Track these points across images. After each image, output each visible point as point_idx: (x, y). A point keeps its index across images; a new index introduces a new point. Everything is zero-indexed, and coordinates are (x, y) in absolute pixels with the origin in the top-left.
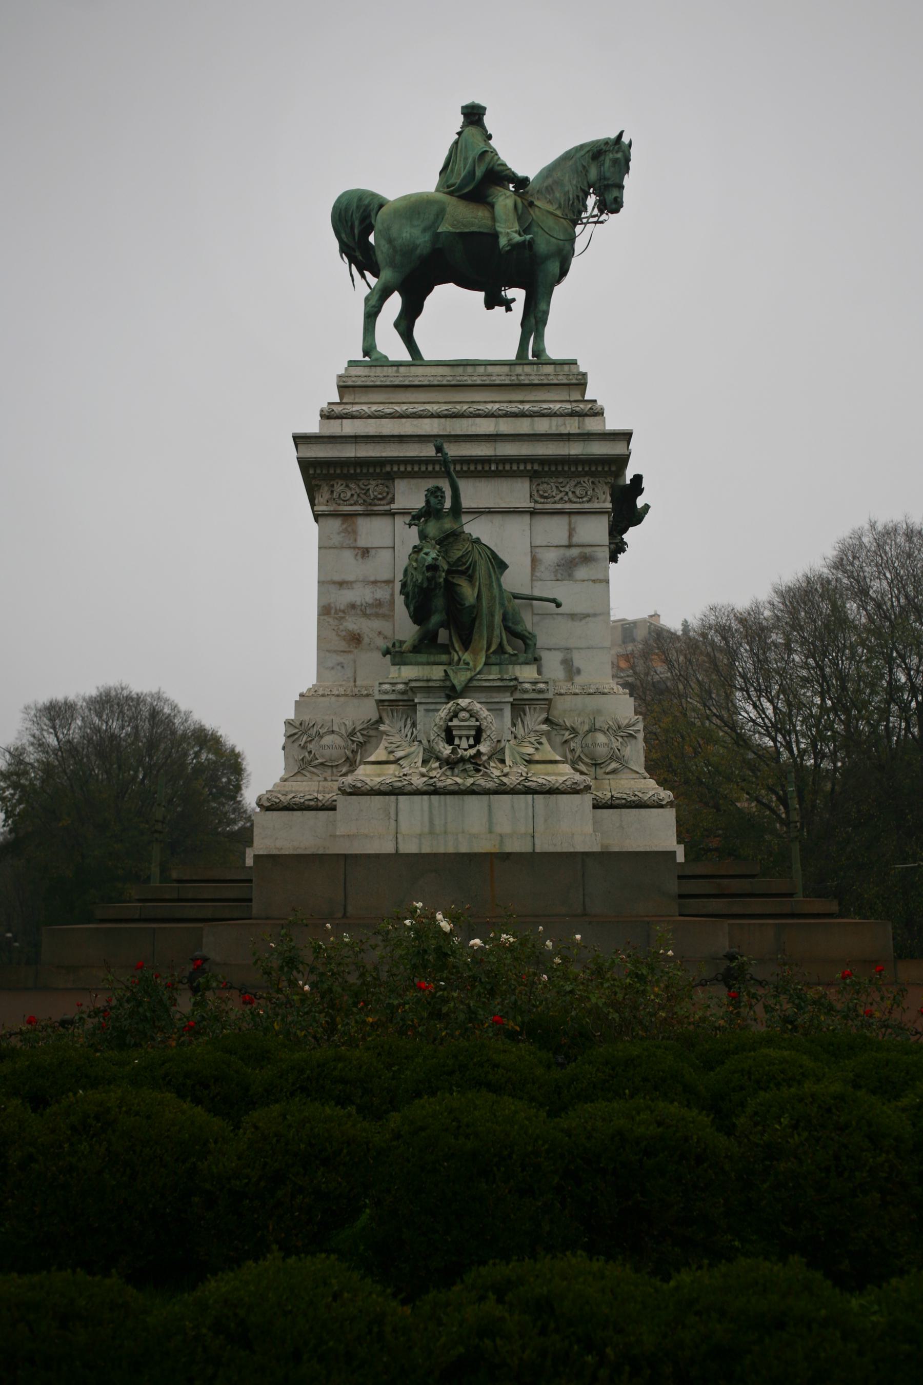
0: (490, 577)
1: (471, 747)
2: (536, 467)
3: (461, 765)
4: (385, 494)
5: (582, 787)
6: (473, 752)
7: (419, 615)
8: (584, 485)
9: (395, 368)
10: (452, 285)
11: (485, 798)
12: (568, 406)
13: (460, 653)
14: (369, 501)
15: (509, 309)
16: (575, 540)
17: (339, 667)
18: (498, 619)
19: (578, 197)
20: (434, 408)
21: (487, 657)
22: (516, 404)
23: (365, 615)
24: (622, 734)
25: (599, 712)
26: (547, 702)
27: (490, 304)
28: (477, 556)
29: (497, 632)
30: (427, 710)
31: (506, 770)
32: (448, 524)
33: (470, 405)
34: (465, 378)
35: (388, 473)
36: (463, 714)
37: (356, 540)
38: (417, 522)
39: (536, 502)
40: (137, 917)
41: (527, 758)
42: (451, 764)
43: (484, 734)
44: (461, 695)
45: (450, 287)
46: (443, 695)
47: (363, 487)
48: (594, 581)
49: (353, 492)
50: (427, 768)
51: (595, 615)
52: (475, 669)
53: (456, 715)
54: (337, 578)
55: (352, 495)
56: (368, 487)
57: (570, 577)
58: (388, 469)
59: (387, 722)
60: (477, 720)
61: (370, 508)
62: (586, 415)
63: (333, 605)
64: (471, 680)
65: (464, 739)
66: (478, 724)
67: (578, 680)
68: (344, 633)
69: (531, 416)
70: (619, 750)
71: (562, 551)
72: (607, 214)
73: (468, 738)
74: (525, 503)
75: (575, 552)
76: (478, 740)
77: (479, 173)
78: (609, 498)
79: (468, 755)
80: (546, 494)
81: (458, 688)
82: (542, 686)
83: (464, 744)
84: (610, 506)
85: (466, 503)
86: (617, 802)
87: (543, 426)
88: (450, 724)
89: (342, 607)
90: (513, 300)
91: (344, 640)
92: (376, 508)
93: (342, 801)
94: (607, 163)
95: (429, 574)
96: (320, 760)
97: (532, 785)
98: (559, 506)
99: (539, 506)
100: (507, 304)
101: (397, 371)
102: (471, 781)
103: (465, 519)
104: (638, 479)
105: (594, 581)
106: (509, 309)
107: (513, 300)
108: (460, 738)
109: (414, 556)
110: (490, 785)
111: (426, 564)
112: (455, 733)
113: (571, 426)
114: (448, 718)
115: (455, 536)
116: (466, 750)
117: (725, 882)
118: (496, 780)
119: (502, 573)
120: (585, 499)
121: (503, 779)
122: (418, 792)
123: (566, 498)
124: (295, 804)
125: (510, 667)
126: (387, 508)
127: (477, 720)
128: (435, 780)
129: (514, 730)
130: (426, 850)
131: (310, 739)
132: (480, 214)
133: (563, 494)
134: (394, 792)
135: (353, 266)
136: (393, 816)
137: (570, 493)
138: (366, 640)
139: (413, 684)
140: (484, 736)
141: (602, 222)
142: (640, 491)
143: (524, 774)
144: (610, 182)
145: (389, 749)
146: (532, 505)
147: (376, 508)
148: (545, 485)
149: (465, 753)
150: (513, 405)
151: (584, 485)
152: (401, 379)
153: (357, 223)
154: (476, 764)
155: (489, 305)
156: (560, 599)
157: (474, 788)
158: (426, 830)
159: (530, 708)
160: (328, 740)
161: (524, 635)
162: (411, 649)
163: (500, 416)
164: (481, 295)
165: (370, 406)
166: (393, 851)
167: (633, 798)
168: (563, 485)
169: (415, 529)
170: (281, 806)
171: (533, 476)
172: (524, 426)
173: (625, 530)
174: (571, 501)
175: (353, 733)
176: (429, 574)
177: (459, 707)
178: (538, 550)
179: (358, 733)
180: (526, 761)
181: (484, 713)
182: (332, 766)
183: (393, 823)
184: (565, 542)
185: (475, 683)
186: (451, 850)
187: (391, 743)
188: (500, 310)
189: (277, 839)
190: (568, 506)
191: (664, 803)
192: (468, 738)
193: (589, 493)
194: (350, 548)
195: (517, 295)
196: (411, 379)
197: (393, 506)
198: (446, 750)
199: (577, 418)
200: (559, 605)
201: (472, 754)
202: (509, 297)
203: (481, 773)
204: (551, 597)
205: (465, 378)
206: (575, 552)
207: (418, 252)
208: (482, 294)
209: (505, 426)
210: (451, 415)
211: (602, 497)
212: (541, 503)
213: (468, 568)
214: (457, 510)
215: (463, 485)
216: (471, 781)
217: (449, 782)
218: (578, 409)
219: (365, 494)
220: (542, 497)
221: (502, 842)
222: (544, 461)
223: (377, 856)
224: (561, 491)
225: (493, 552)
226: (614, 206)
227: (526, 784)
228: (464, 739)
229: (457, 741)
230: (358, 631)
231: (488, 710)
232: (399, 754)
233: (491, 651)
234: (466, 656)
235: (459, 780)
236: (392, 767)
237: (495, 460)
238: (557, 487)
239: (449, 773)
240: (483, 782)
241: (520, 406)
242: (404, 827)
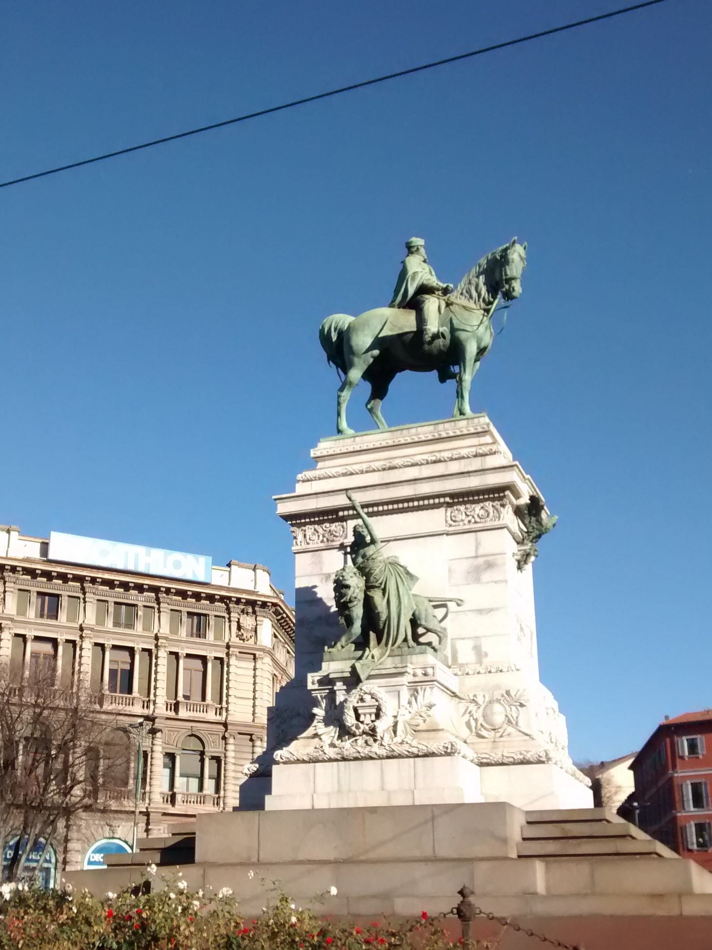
8: (486, 508)
9: (352, 439)
10: (398, 374)
11: (379, 761)
16: (481, 551)
21: (392, 650)
27: (442, 379)
37: (321, 569)
39: (451, 526)
40: (130, 863)
45: (407, 373)
47: (325, 529)
48: (496, 582)
51: (497, 609)
57: (478, 580)
61: (330, 543)
65: (368, 716)
66: (377, 704)
67: (486, 661)
71: (471, 561)
73: (371, 715)
74: (442, 527)
75: (481, 561)
76: (378, 716)
98: (467, 527)
101: (354, 441)
102: (368, 748)
105: (496, 582)
108: (365, 715)
110: (383, 752)
112: (360, 711)
113: (476, 464)
118: (387, 748)
122: (330, 760)
125: (409, 656)
130: (334, 805)
134: (315, 761)
135: (339, 369)
155: (442, 379)
156: (462, 598)
161: (436, 630)
163: (422, 464)
164: (435, 373)
166: (309, 807)
174: (476, 522)
177: (362, 691)
181: (381, 694)
183: (312, 784)
184: (473, 554)
192: (371, 715)
194: (317, 575)
199: (480, 458)
206: (481, 561)
209: (427, 471)
212: (454, 526)
221: (389, 799)
222: (452, 495)
225: (405, 568)
228: (368, 716)
231: (387, 692)
235: (360, 749)
240: (376, 748)
242: (319, 788)
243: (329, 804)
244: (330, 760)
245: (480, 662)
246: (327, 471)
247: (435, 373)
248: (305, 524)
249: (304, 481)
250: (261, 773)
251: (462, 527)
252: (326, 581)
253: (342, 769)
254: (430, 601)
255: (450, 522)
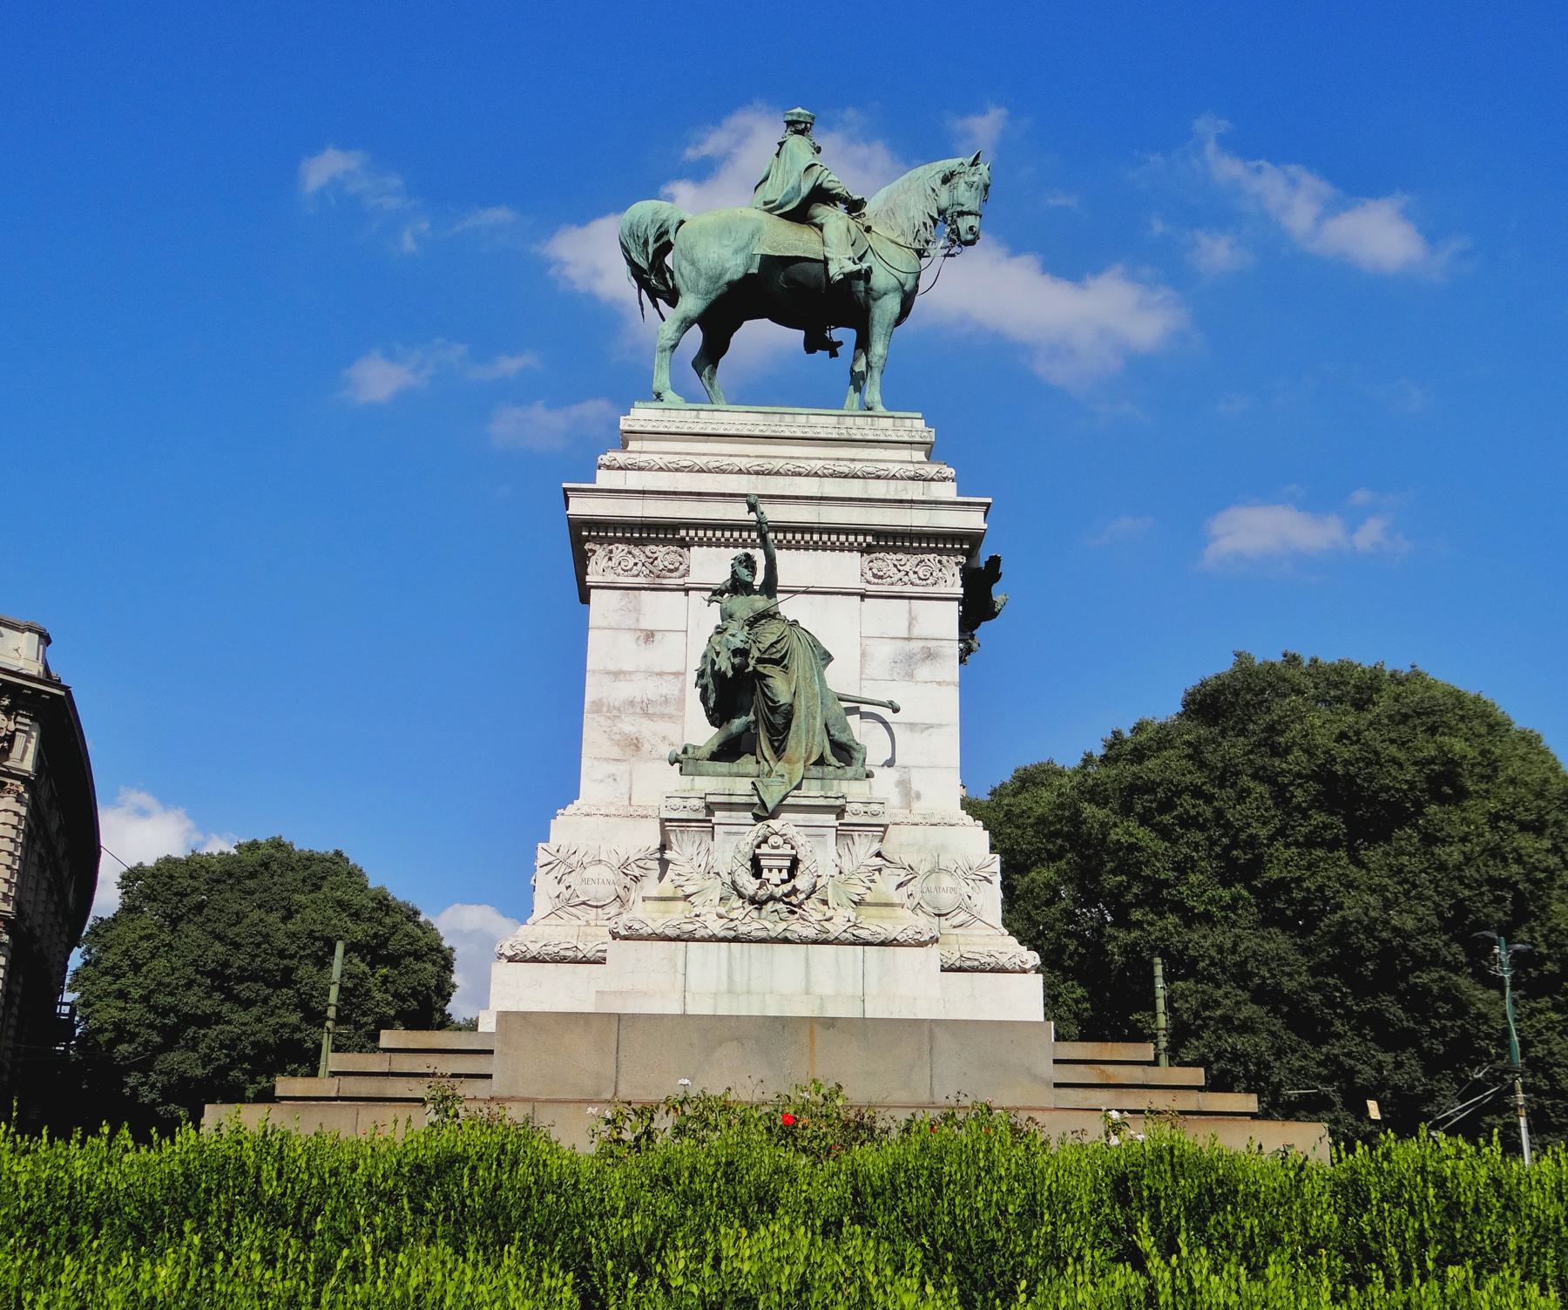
0: (812, 669)
1: (784, 882)
2: (869, 539)
3: (771, 904)
4: (677, 565)
5: (927, 938)
6: (787, 888)
7: (718, 715)
8: (929, 563)
10: (766, 320)
12: (910, 467)
13: (771, 763)
14: (656, 571)
15: (834, 354)
16: (916, 632)
17: (610, 780)
18: (819, 723)
19: (925, 224)
20: (743, 463)
22: (846, 463)
23: (646, 714)
24: (974, 877)
25: (944, 848)
26: (882, 829)
28: (795, 643)
29: (817, 739)
30: (729, 833)
31: (829, 913)
32: (760, 603)
33: (788, 461)
34: (782, 429)
35: (683, 539)
36: (772, 840)
37: (638, 620)
38: (719, 598)
39: (868, 582)
41: (856, 899)
42: (758, 903)
43: (800, 866)
44: (774, 815)
46: (749, 815)
47: (650, 555)
48: (939, 683)
49: (637, 561)
50: (727, 908)
51: (940, 726)
52: (791, 784)
53: (765, 841)
54: (612, 667)
55: (636, 564)
56: (655, 555)
57: (910, 676)
58: (683, 533)
59: (675, 847)
60: (793, 848)
61: (658, 581)
62: (932, 480)
63: (605, 701)
64: (785, 797)
65: (775, 871)
66: (794, 852)
67: (917, 806)
68: (618, 737)
69: (864, 478)
70: (970, 897)
71: (900, 643)
72: (959, 246)
73: (780, 871)
74: (857, 584)
75: (916, 646)
76: (792, 872)
77: (805, 190)
78: (960, 582)
79: (781, 893)
80: (881, 574)
81: (770, 806)
82: (875, 807)
83: (775, 877)
84: (961, 591)
85: (783, 580)
86: (969, 963)
87: (878, 489)
88: (757, 851)
89: (617, 704)
90: (840, 343)
91: (618, 745)
92: (664, 581)
93: (615, 949)
94: (962, 187)
95: (737, 661)
96: (582, 899)
97: (864, 934)
98: (897, 588)
99: (869, 587)
100: (832, 348)
101: (697, 417)
102: (783, 925)
103: (780, 597)
104: (994, 562)
105: (939, 683)
106: (834, 354)
107: (840, 343)
108: (770, 870)
109: (718, 638)
110: (810, 933)
111: (732, 648)
112: (763, 863)
114: (755, 843)
115: (769, 615)
116: (777, 886)
117: (1110, 1069)
119: (825, 666)
120: (928, 582)
121: (826, 924)
122: (714, 939)
123: (906, 579)
124: (547, 954)
125: (836, 782)
126: (681, 581)
127: (793, 848)
128: (736, 922)
129: (838, 862)
130: (723, 1010)
131: (568, 870)
132: (806, 236)
133: (904, 573)
136: (681, 969)
137: (911, 573)
138: (646, 747)
139: (710, 799)
140: (801, 866)
141: (953, 255)
142: (997, 577)
143: (852, 919)
144: (965, 209)
145: (677, 883)
146: (864, 585)
147: (664, 581)
148: (880, 562)
149: (776, 889)
150: (841, 463)
151: (929, 563)
152: (702, 425)
153: (651, 240)
154: (790, 903)
155: (810, 346)
156: (897, 702)
157: (788, 935)
158: (724, 987)
159: (859, 835)
160: (592, 872)
162: (708, 756)
164: (800, 335)
165: (661, 456)
166: (679, 1011)
167: (988, 960)
168: (903, 563)
169: (716, 607)
170: (528, 957)
171: (867, 550)
172: (855, 488)
173: (976, 627)
175: (625, 866)
176: (737, 661)
177: (769, 829)
178: (869, 642)
179: (633, 864)
180: (855, 903)
181: (800, 839)
182: (597, 907)
183: (680, 978)
185: (789, 801)
186: (755, 1012)
187: (679, 875)
188: (822, 355)
189: (521, 999)
190: (909, 589)
191: (1027, 966)
192: (780, 871)
193: (934, 574)
195: (844, 335)
196: (714, 426)
197: (687, 579)
198: (750, 885)
200: (896, 710)
201: (786, 891)
202: (835, 339)
203: (797, 916)
204: (885, 700)
205: (782, 429)
206: (916, 646)
207: (727, 278)
208: (801, 334)
210: (763, 472)
211: (950, 579)
213: (783, 657)
214: (770, 587)
215: (782, 557)
216: (783, 925)
217: (755, 925)
218: (922, 472)
219: (652, 563)
220: (875, 576)
221: (822, 1007)
223: (661, 1017)
224: (899, 571)
225: (814, 639)
226: (970, 237)
227: (855, 932)
228: (775, 871)
229: (765, 874)
230: (637, 735)
232: (689, 890)
233: (811, 762)
234: (780, 767)
236: (681, 905)
237: (819, 528)
238: (895, 566)
239: (755, 914)
240: (798, 928)
241: (852, 466)
243: (715, 1011)
244: (714, 939)
245: (909, 806)
246: (656, 457)
247: (800, 335)
248: (612, 541)
249: (608, 468)
250: (534, 957)
251: (884, 588)
252: (645, 643)
253: (753, 952)
254: (840, 700)
255: (869, 576)
